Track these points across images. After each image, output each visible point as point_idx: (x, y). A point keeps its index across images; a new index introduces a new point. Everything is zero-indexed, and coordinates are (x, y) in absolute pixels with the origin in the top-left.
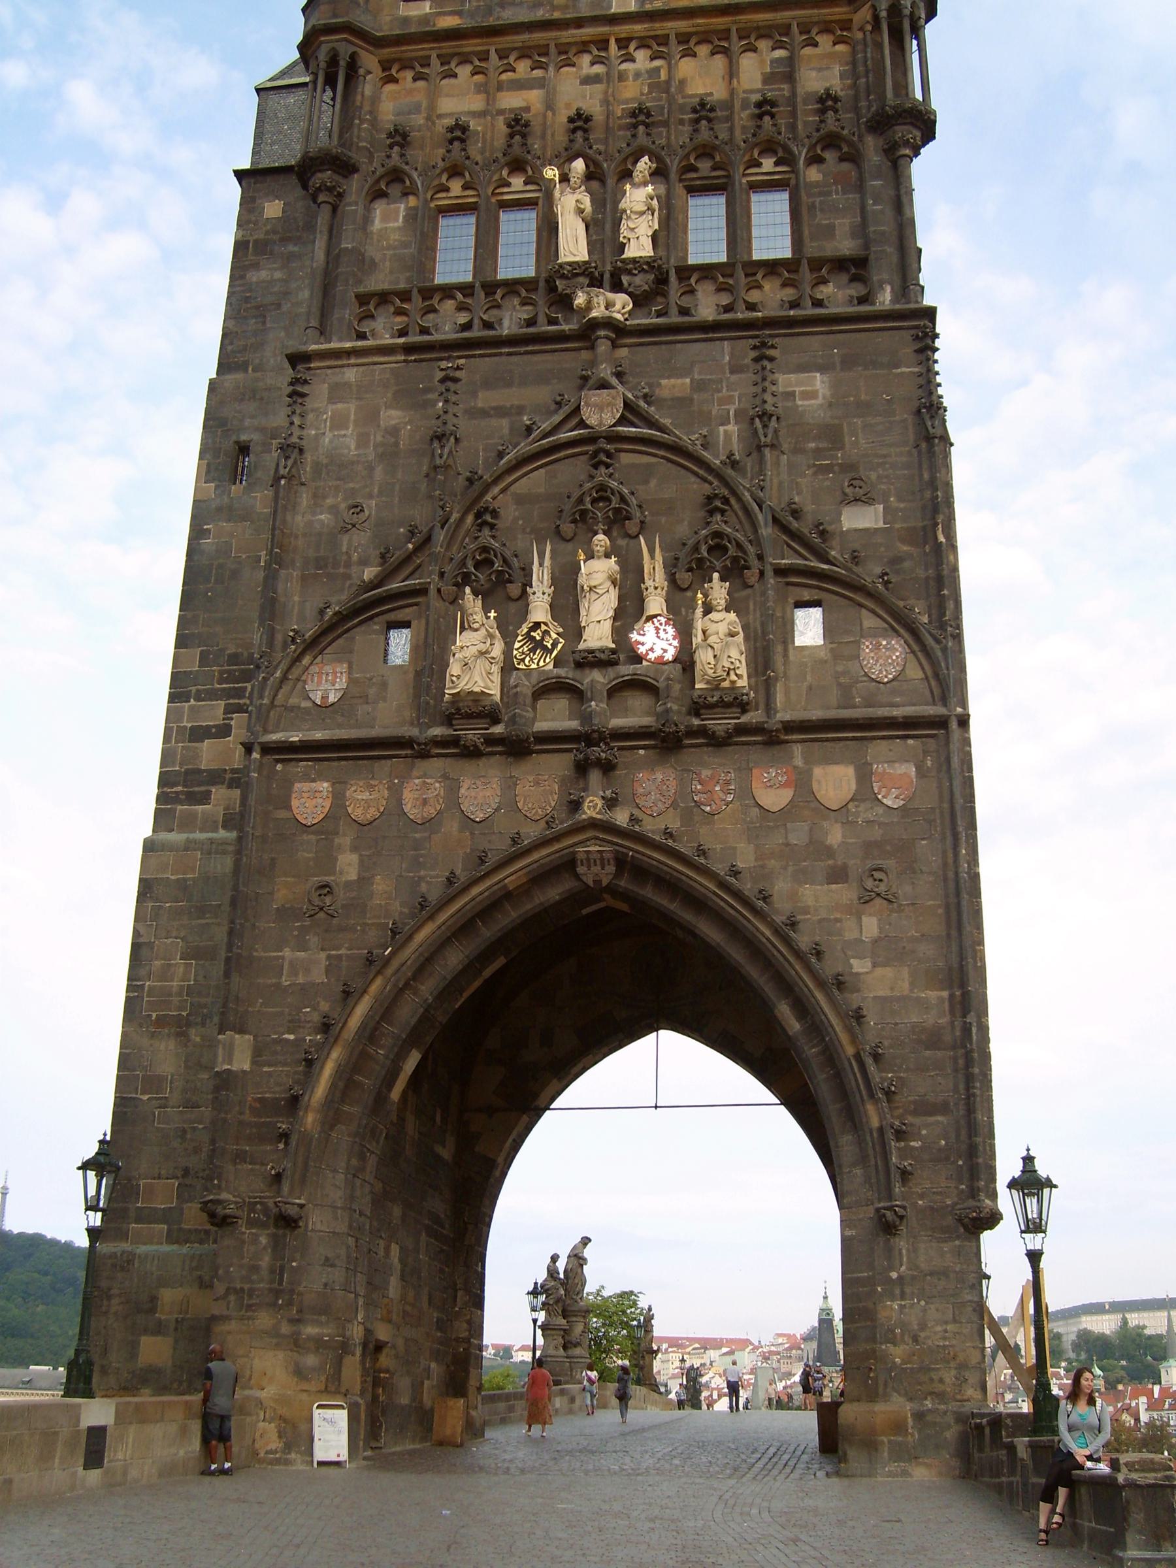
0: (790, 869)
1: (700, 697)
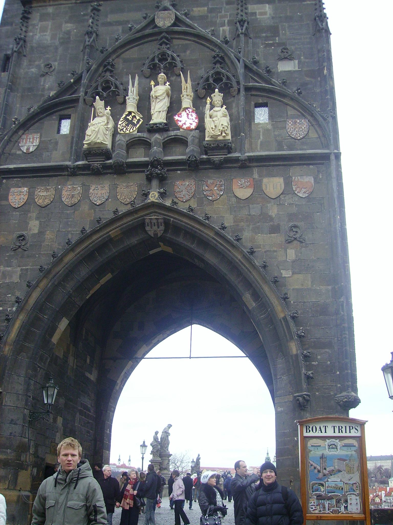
0: (251, 227)
1: (207, 144)
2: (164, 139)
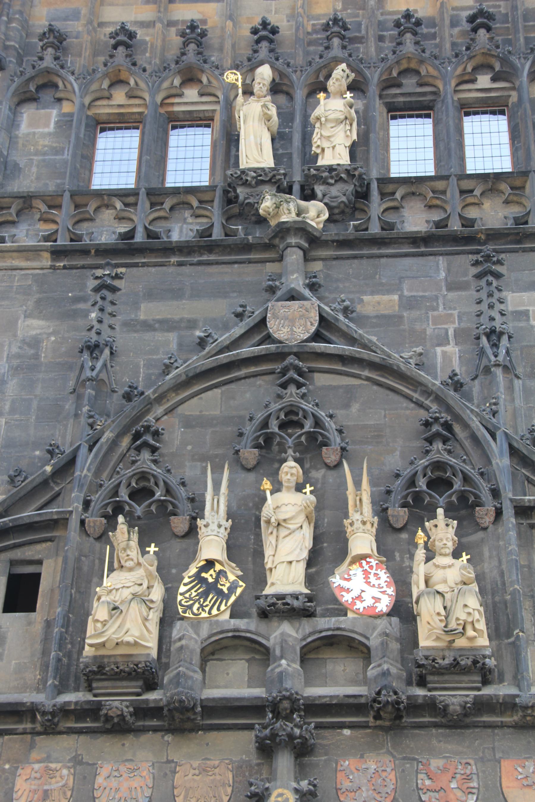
1: (427, 658)
2: (304, 639)
